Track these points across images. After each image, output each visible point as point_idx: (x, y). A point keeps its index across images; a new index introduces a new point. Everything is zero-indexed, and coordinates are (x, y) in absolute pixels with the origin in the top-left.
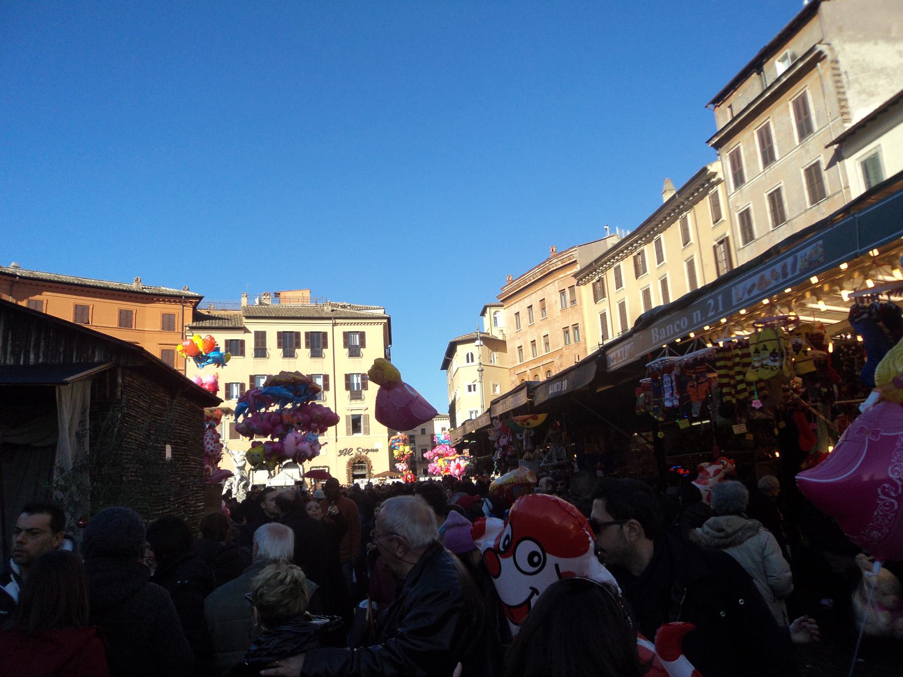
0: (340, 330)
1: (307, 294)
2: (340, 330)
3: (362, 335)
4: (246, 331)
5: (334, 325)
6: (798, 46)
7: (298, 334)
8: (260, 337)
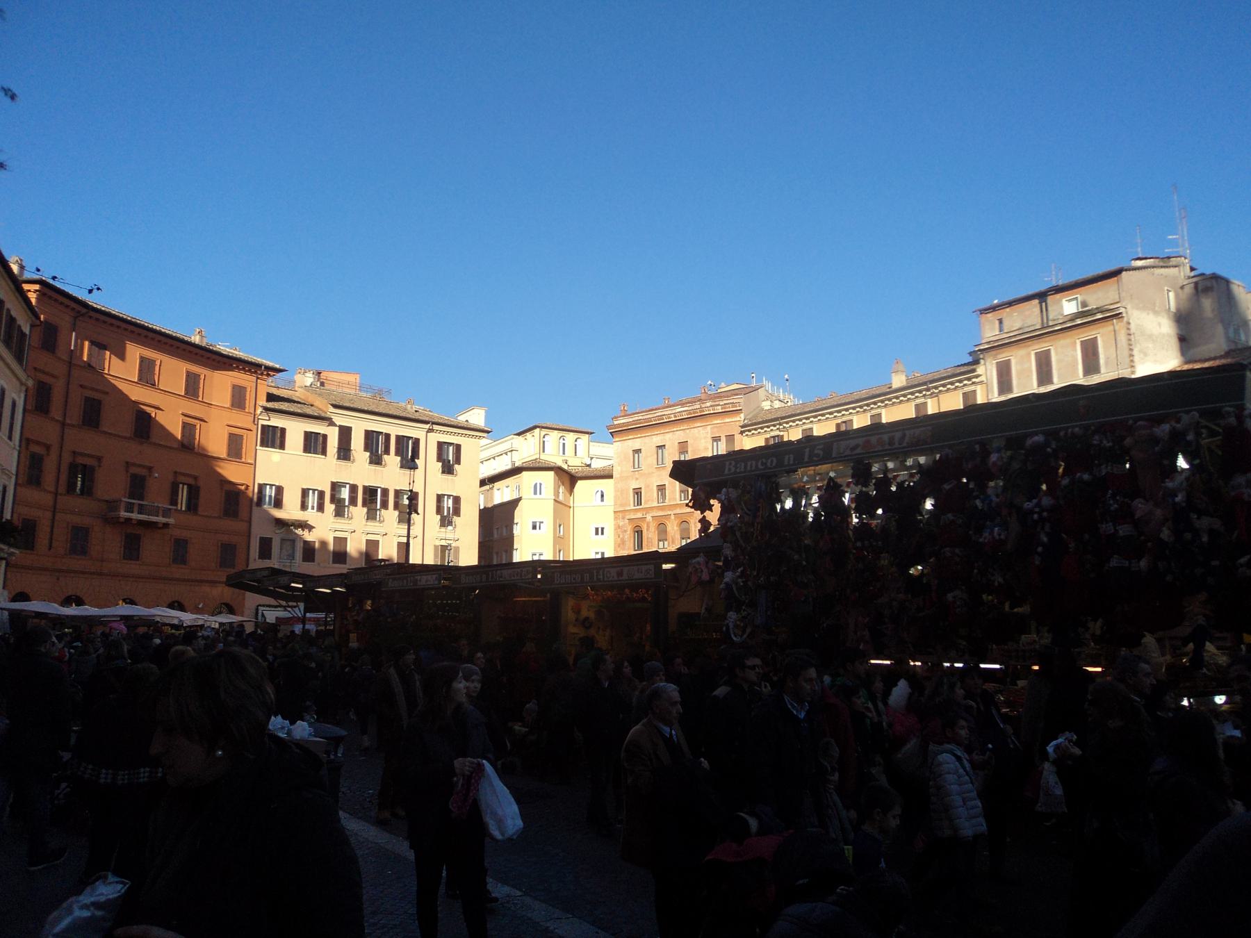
0: (434, 438)
1: (358, 377)
2: (434, 438)
3: (458, 448)
4: (331, 423)
5: (430, 430)
6: (1097, 297)
7: (388, 436)
8: (345, 433)
